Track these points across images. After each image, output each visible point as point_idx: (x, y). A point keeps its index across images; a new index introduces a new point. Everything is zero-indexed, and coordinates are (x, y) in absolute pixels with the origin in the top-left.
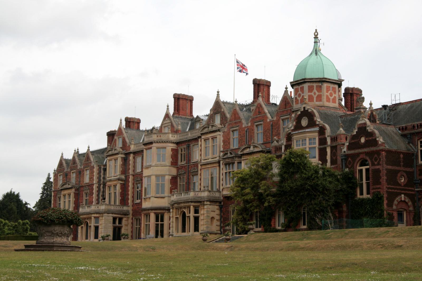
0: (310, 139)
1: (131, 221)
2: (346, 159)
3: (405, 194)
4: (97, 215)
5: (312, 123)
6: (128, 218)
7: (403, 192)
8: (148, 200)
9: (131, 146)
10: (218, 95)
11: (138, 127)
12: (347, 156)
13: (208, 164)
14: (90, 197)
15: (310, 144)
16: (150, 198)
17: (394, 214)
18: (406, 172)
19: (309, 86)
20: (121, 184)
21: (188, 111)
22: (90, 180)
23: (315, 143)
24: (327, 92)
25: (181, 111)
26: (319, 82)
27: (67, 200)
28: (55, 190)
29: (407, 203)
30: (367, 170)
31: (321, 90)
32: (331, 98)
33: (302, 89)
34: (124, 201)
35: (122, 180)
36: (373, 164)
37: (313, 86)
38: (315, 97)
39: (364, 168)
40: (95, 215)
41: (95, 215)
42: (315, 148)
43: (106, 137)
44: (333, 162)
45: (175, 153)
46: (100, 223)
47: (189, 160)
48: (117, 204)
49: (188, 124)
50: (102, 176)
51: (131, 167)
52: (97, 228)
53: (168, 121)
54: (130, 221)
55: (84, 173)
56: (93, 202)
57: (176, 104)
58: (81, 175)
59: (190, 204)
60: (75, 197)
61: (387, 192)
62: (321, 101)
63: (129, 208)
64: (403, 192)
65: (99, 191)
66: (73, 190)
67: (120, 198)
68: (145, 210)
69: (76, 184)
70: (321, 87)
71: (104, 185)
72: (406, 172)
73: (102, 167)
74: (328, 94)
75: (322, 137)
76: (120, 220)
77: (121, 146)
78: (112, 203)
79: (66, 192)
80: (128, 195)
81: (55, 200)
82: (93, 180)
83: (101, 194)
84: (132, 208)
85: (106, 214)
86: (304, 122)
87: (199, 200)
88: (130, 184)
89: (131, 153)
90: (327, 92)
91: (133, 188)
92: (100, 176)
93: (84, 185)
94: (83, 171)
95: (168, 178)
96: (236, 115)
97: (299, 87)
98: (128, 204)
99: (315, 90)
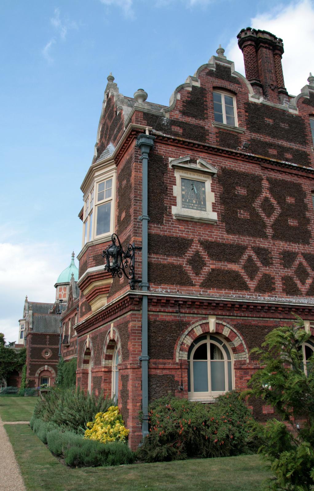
3: (48, 365)
7: (46, 363)
17: (36, 381)
18: (52, 349)
29: (50, 372)
31: (66, 290)
38: (62, 295)
61: (30, 364)
64: (46, 363)
70: (66, 288)
72: (52, 349)
99: (63, 291)
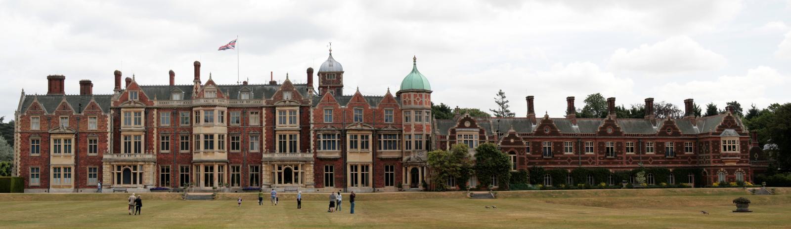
0: (475, 135)
4: (142, 163)
9: (154, 102)
10: (287, 76)
12: (502, 148)
13: (286, 130)
16: (213, 152)
28: (25, 131)
30: (515, 157)
36: (520, 154)
39: (512, 156)
51: (155, 120)
52: (141, 174)
53: (213, 87)
55: (87, 120)
59: (299, 162)
87: (305, 160)
88: (155, 136)
89: (156, 108)
93: (85, 131)
94: (85, 117)
95: (226, 136)
96: (330, 98)
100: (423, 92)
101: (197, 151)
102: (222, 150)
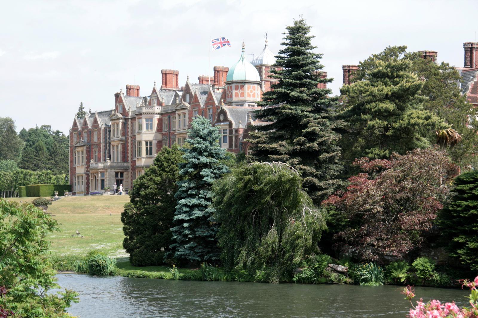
1: (131, 174)
2: (242, 145)
4: (103, 171)
5: (226, 119)
6: (128, 172)
8: (140, 159)
11: (138, 94)
12: (242, 143)
13: (180, 134)
14: (99, 154)
15: (224, 133)
19: (235, 86)
20: (122, 144)
21: (174, 84)
22: (98, 140)
23: (226, 133)
24: (248, 90)
25: (168, 84)
26: (242, 83)
27: (80, 156)
32: (251, 94)
33: (231, 87)
34: (125, 158)
35: (123, 141)
37: (238, 86)
40: (101, 171)
41: (101, 171)
42: (227, 136)
43: (115, 98)
44: (236, 146)
45: (160, 121)
46: (106, 177)
47: (170, 129)
48: (119, 161)
49: (172, 96)
50: (108, 136)
52: (103, 181)
53: (155, 95)
54: (130, 175)
56: (101, 158)
57: (164, 78)
58: (92, 134)
60: (87, 153)
62: (243, 96)
63: (129, 164)
65: (105, 149)
66: (85, 148)
67: (122, 156)
68: (138, 167)
69: (88, 142)
70: (243, 86)
71: (110, 143)
73: (108, 129)
74: (249, 91)
75: (230, 129)
76: (122, 174)
77: (122, 112)
78: (116, 161)
79: (79, 149)
80: (128, 153)
81: (72, 155)
82: (100, 140)
83: (107, 151)
84: (131, 164)
85: (109, 170)
86: (222, 118)
88: (129, 144)
89: (129, 118)
90: (248, 90)
91: (132, 148)
92: (106, 136)
95: (154, 143)
97: (229, 86)
98: (128, 160)
100: (233, 83)
101: (139, 157)
102: (149, 156)
